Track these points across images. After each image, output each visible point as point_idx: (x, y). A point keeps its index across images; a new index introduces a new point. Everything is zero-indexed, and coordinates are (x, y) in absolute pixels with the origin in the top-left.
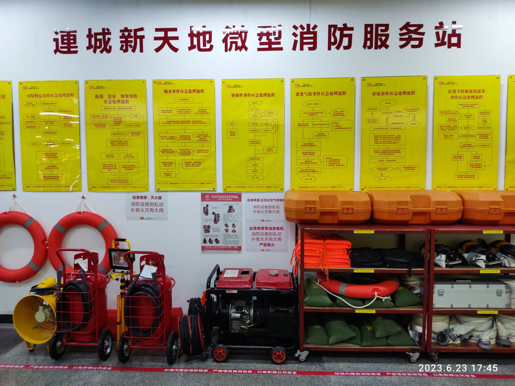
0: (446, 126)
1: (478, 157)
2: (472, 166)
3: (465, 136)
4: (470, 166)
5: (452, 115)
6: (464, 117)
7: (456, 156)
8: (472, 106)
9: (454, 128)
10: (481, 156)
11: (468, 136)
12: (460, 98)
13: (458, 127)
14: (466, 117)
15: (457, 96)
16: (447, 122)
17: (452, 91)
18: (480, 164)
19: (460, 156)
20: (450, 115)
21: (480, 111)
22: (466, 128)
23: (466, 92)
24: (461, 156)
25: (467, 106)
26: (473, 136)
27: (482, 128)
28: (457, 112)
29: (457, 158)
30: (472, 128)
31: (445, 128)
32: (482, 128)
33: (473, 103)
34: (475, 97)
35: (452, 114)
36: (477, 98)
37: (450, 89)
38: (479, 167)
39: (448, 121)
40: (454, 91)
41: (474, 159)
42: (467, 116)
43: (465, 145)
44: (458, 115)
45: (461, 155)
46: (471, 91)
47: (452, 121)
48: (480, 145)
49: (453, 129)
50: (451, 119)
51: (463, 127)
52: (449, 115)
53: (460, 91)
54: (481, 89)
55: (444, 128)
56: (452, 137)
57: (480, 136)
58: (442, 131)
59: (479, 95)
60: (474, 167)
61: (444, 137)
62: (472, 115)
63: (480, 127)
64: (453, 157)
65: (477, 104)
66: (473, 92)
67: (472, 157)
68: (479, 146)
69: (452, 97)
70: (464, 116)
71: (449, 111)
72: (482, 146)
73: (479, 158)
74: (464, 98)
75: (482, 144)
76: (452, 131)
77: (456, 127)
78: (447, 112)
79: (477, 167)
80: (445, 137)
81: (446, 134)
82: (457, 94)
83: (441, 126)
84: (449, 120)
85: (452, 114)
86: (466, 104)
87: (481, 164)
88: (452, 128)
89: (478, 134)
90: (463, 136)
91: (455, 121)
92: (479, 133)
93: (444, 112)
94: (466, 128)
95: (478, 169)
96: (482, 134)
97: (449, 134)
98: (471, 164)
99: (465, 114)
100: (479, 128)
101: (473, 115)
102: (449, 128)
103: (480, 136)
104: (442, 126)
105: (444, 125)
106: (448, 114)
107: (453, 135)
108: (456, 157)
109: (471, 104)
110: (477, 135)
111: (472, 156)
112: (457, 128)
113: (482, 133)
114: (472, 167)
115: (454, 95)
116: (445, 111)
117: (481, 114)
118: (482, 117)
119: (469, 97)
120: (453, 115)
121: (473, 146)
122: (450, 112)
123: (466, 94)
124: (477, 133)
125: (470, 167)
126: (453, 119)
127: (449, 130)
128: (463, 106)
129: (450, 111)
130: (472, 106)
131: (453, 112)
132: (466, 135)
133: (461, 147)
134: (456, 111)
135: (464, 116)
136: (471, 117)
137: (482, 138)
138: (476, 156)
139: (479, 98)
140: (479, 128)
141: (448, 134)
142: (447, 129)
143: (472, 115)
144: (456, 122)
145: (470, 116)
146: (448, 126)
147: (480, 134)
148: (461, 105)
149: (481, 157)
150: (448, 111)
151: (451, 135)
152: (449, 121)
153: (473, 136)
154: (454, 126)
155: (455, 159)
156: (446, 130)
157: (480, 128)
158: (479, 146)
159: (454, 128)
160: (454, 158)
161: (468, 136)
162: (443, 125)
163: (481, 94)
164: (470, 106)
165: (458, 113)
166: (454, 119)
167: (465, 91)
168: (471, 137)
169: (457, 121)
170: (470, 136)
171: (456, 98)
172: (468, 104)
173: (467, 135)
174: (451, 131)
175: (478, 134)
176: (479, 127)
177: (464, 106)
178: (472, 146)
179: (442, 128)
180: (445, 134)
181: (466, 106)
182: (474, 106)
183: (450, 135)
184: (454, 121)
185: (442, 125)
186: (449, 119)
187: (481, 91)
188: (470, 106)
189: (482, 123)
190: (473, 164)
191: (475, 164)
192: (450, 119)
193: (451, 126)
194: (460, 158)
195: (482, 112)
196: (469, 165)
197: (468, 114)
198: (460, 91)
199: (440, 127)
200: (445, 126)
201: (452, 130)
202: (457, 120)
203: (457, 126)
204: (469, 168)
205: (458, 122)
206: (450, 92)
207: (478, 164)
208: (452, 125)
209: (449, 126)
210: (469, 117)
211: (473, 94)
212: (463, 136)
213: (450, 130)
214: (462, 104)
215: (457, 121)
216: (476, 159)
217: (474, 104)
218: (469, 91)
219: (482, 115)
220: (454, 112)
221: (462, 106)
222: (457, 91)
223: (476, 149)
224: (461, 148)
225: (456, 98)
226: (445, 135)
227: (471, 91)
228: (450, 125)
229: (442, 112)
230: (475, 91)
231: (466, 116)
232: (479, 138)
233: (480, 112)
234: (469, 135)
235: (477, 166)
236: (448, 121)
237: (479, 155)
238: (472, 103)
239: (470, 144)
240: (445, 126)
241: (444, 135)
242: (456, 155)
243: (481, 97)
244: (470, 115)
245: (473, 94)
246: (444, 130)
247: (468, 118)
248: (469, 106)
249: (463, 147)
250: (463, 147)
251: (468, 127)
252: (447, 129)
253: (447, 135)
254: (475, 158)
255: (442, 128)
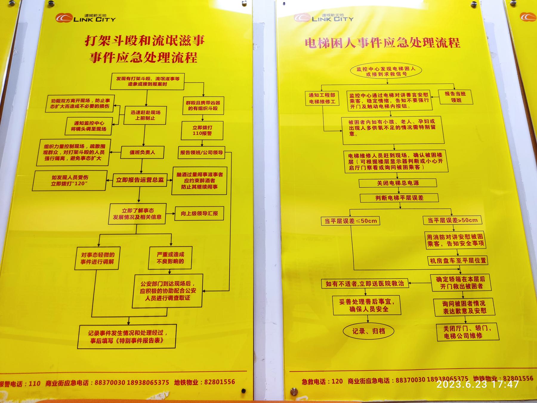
0: (67, 146)
1: (176, 254)
2: (154, 291)
3: (131, 180)
4: (142, 291)
5: (89, 109)
6: (131, 118)
7: (90, 255)
8: (161, 82)
9: (91, 152)
10: (187, 252)
11: (143, 180)
12: (122, 58)
13: (106, 150)
14: (140, 116)
15: (111, 54)
16: (69, 131)
17: (97, 39)
18: (183, 283)
19: (107, 254)
20: (84, 109)
21: (186, 99)
22: (137, 152)
23: (141, 41)
24: (112, 254)
25: (145, 84)
26: (161, 180)
27: (193, 152)
28: (108, 100)
29: (94, 262)
30: (159, 152)
31: (61, 152)
32: (193, 152)
33: (166, 76)
34: (171, 58)
35: (92, 106)
36: (178, 58)
37: (92, 35)
38: (182, 298)
39: (73, 129)
40: (105, 40)
41: (162, 266)
42: (143, 112)
43: (130, 210)
44: (110, 109)
45: (109, 250)
46: (159, 41)
47: (89, 129)
48: (186, 210)
49: (88, 155)
50: (87, 123)
51: (126, 152)
52: (80, 109)
53: (123, 39)
54: (193, 34)
55: (56, 153)
56: (83, 184)
57: (186, 181)
58: (50, 162)
59: (184, 50)
60: (159, 298)
61: (53, 184)
62: (159, 113)
63: (185, 149)
64: (80, 258)
65: (178, 79)
66: (164, 42)
67: (154, 257)
68: (183, 213)
69: (96, 57)
70: (133, 112)
71: (81, 97)
72: (194, 213)
73: (182, 261)
74: (134, 61)
75: (191, 210)
76: (85, 162)
77: (99, 150)
78: (73, 101)
79: (170, 298)
80: (58, 184)
81: (62, 174)
82: (114, 48)
83: (46, 146)
84: (78, 127)
85: (92, 106)
86: (141, 76)
87: (188, 283)
88: (86, 152)
89: (179, 175)
90: (125, 180)
91: (99, 129)
92: (182, 171)
93: (63, 101)
94: (137, 152)
95: (173, 303)
96: (195, 174)
97: (72, 174)
98: (149, 284)
99: (136, 109)
100: (183, 152)
101: (163, 111)
102: (76, 152)
103: (186, 181)
104: (51, 146)
105: (59, 143)
106: (77, 106)
107: (86, 177)
108: (92, 258)
109: (158, 79)
110: (175, 178)
111: (154, 251)
112: (102, 152)
113: (192, 170)
114: (150, 295)
115: (103, 50)
116: (66, 98)
117: (190, 108)
118: (196, 117)
119: (150, 58)
120: (94, 109)
121: (159, 217)
122: (83, 100)
123: (143, 50)
124: (177, 171)
125: (145, 295)
126: (92, 123)
127: (73, 158)
128: (130, 84)
129: (86, 97)
130: (160, 84)
131: (93, 101)
132: (135, 176)
133: (115, 217)
134: (105, 98)
135: (133, 112)
136: (156, 116)
137: (194, 187)
138: (171, 254)
139: (184, 58)
140: (183, 152)
141: (68, 174)
142: (68, 157)
143: (159, 113)
144: (102, 132)
145: (151, 116)
146: (71, 146)
147: (185, 174)
148: (124, 79)
149: (187, 258)
150: (75, 97)
151: (80, 177)
152: (78, 129)
153: (161, 180)
154: (92, 146)
155: (86, 266)
156: (63, 158)
157: (188, 152)
158: (183, 213)
159: (91, 152)
160: (83, 262)
161: (143, 180)
162: (54, 143)
163: (192, 48)
164: (155, 84)
165: (111, 104)
166: (97, 123)
167: (138, 41)
168: (152, 184)
169: (104, 129)
170: (149, 180)
171: (108, 60)
172: (148, 78)
173: (140, 176)
174: (81, 162)
175: (179, 175)
176: (181, 149)
177: (135, 84)
178: (154, 217)
179: (51, 152)
180: (57, 174)
181: (140, 84)
182: (169, 82)
183: (75, 177)
184: (94, 129)
185: (49, 143)
186: (77, 123)
187: (192, 39)
188: (155, 84)
189: (196, 137)
190: (155, 283)
191: (165, 283)
192: (81, 123)
193: (82, 146)
194: (106, 262)
195: (193, 103)
196: (138, 287)
197: (146, 109)
198: (123, 39)
199: (42, 149)
200: (62, 146)
201: (83, 158)
202: (107, 123)
203: (103, 146)
204: (141, 300)
205: (108, 132)
206: (91, 42)
207: (177, 283)
208: (87, 145)
209: (77, 146)
210: (148, 118)
211: (166, 48)
212: (125, 180)
213: (78, 158)
214: (126, 76)
215: (104, 129)
216: (168, 266)
217: (168, 79)
218: (152, 41)
219: (194, 112)
220: (97, 100)
221: (127, 82)
222: (112, 40)
223: (171, 225)
224: (112, 221)
225: (108, 60)
226: (59, 177)
227: (159, 41)
228: (80, 142)
229: (58, 101)
230: (172, 40)
231: (138, 112)
232: (183, 187)
233: (188, 103)
234: (146, 176)
235: (171, 291)
236: (73, 129)
237: (179, 250)
238: (160, 76)
239: (149, 207)
240: (62, 146)
241: (54, 177)
242: (93, 251)
243: (191, 57)
244: (153, 112)
245: (166, 48)
246: (57, 158)
247: (145, 122)
248: (150, 84)
249: (121, 217)
250: (121, 217)
251: (145, 149)
252: (68, 157)
253: (65, 177)
254: (165, 261)
255: (51, 152)
